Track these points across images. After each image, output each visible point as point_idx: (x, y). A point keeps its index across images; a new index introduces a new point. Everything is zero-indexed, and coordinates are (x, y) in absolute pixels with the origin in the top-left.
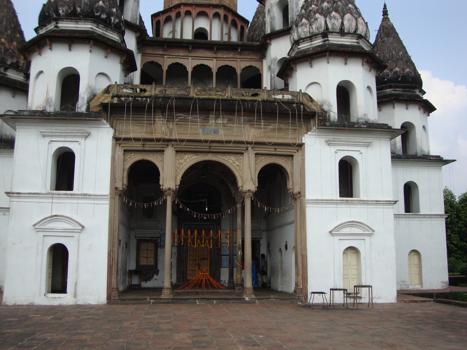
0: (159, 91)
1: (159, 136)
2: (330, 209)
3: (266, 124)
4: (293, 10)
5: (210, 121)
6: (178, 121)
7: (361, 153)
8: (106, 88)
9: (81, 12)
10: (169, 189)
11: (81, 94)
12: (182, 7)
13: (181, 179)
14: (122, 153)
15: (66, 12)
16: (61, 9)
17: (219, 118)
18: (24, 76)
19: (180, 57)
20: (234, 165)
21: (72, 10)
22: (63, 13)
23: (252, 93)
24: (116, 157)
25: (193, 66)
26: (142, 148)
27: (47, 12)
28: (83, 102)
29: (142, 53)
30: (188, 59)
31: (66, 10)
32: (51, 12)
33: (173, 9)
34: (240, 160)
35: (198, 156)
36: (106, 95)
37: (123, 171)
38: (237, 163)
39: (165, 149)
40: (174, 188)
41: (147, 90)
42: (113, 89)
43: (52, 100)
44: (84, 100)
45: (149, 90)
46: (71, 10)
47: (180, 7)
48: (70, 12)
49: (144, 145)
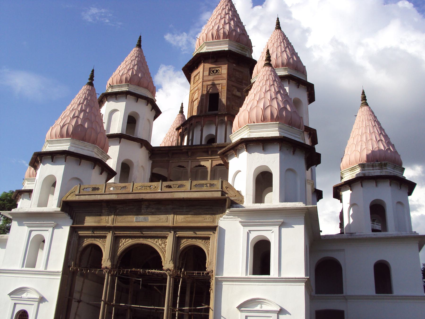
1: (103, 224)
2: (237, 287)
3: (187, 210)
5: (143, 211)
6: (118, 212)
7: (273, 232)
10: (106, 268)
12: (193, 119)
13: (118, 260)
14: (77, 239)
17: (149, 207)
19: (181, 161)
20: (161, 247)
23: (178, 185)
24: (72, 242)
25: (192, 167)
26: (91, 234)
29: (153, 161)
30: (188, 161)
33: (188, 122)
34: (165, 243)
35: (133, 240)
37: (77, 253)
38: (163, 245)
39: (107, 235)
40: (110, 267)
47: (192, 119)
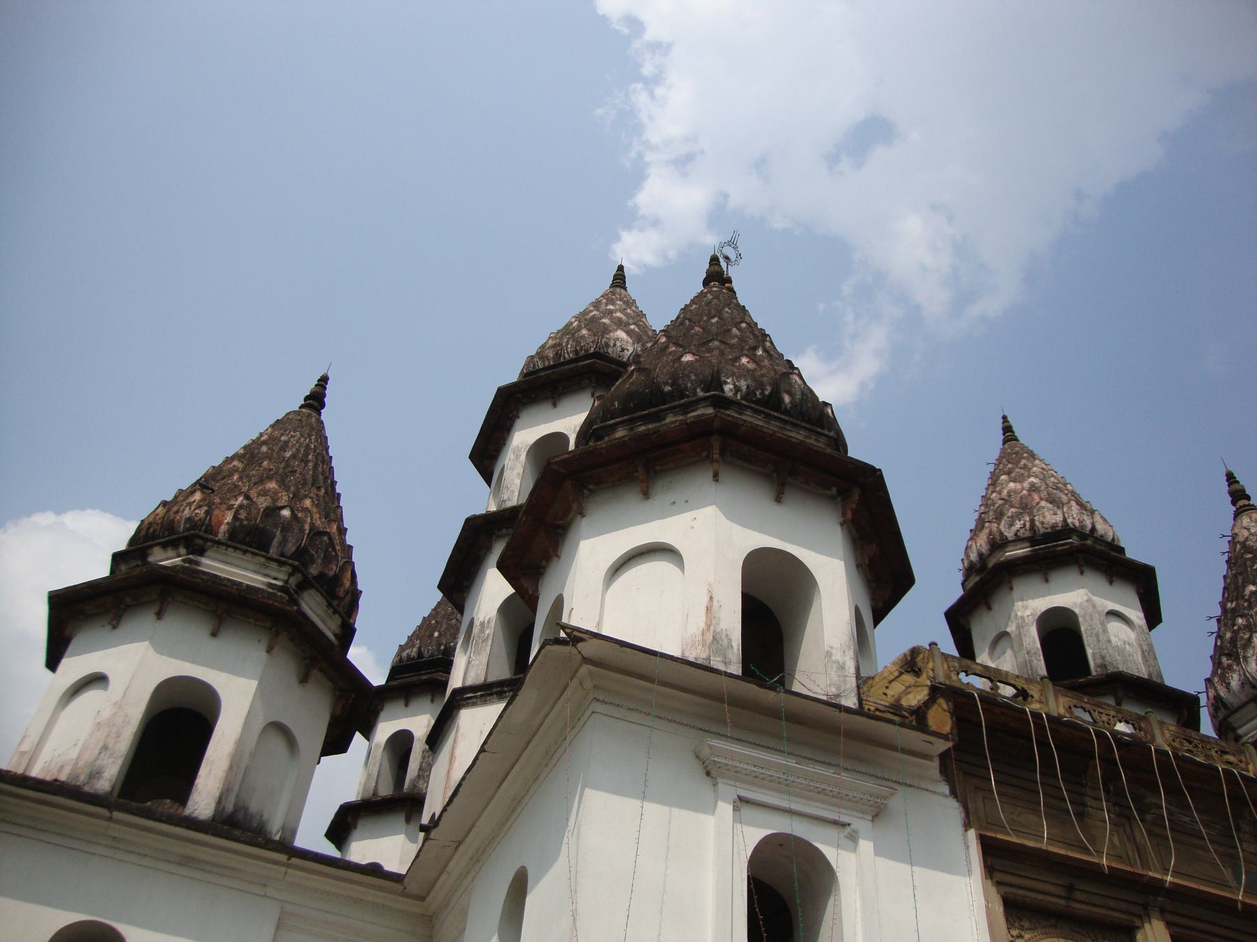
0: (1067, 706)
4: (1097, 635)
8: (905, 655)
9: (791, 408)
11: (833, 651)
15: (747, 394)
16: (728, 381)
18: (338, 631)
21: (767, 393)
22: (736, 394)
27: (666, 384)
28: (845, 681)
31: (748, 387)
32: (689, 385)
36: (908, 678)
41: (1032, 697)
42: (930, 665)
43: (730, 641)
44: (846, 674)
45: (1036, 696)
46: (762, 393)
48: (758, 396)
49: (1070, 889)
